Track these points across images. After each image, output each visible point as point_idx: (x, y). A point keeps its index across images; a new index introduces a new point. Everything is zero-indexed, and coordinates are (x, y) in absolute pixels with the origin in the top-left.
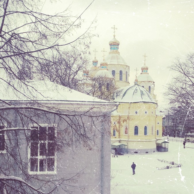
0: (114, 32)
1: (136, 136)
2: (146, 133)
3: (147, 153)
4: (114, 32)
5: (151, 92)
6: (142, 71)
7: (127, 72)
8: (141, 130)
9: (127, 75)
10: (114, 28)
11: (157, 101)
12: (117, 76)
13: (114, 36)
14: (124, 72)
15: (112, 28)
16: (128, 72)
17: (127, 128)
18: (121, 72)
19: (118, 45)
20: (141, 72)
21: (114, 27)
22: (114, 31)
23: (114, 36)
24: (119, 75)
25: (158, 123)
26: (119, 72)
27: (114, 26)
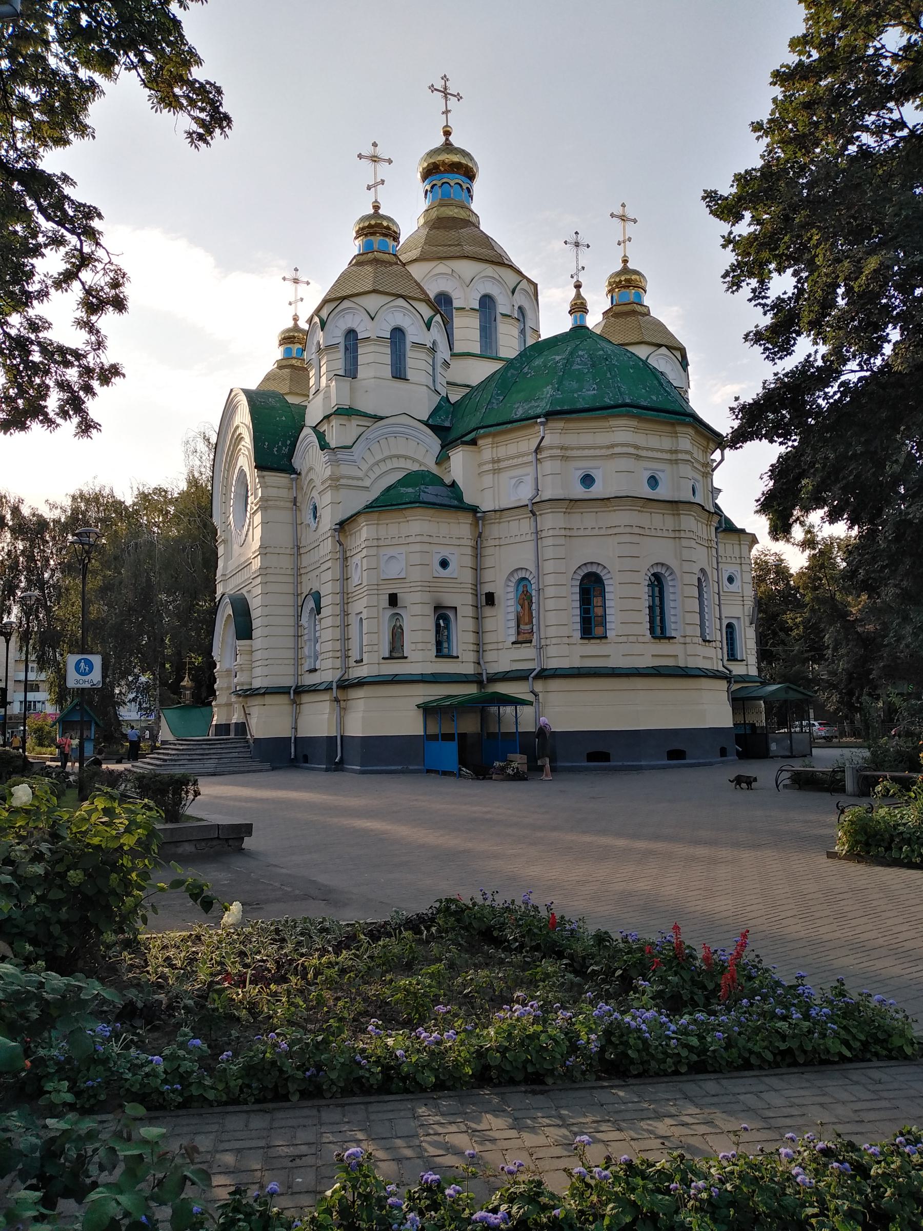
0: (447, 112)
1: (593, 647)
2: (659, 628)
3: (676, 755)
4: (447, 112)
8: (625, 606)
10: (445, 93)
13: (447, 133)
14: (503, 305)
15: (433, 88)
16: (529, 313)
18: (487, 302)
19: (470, 174)
21: (446, 88)
22: (444, 109)
23: (447, 133)
24: (474, 322)
25: (731, 580)
27: (444, 78)
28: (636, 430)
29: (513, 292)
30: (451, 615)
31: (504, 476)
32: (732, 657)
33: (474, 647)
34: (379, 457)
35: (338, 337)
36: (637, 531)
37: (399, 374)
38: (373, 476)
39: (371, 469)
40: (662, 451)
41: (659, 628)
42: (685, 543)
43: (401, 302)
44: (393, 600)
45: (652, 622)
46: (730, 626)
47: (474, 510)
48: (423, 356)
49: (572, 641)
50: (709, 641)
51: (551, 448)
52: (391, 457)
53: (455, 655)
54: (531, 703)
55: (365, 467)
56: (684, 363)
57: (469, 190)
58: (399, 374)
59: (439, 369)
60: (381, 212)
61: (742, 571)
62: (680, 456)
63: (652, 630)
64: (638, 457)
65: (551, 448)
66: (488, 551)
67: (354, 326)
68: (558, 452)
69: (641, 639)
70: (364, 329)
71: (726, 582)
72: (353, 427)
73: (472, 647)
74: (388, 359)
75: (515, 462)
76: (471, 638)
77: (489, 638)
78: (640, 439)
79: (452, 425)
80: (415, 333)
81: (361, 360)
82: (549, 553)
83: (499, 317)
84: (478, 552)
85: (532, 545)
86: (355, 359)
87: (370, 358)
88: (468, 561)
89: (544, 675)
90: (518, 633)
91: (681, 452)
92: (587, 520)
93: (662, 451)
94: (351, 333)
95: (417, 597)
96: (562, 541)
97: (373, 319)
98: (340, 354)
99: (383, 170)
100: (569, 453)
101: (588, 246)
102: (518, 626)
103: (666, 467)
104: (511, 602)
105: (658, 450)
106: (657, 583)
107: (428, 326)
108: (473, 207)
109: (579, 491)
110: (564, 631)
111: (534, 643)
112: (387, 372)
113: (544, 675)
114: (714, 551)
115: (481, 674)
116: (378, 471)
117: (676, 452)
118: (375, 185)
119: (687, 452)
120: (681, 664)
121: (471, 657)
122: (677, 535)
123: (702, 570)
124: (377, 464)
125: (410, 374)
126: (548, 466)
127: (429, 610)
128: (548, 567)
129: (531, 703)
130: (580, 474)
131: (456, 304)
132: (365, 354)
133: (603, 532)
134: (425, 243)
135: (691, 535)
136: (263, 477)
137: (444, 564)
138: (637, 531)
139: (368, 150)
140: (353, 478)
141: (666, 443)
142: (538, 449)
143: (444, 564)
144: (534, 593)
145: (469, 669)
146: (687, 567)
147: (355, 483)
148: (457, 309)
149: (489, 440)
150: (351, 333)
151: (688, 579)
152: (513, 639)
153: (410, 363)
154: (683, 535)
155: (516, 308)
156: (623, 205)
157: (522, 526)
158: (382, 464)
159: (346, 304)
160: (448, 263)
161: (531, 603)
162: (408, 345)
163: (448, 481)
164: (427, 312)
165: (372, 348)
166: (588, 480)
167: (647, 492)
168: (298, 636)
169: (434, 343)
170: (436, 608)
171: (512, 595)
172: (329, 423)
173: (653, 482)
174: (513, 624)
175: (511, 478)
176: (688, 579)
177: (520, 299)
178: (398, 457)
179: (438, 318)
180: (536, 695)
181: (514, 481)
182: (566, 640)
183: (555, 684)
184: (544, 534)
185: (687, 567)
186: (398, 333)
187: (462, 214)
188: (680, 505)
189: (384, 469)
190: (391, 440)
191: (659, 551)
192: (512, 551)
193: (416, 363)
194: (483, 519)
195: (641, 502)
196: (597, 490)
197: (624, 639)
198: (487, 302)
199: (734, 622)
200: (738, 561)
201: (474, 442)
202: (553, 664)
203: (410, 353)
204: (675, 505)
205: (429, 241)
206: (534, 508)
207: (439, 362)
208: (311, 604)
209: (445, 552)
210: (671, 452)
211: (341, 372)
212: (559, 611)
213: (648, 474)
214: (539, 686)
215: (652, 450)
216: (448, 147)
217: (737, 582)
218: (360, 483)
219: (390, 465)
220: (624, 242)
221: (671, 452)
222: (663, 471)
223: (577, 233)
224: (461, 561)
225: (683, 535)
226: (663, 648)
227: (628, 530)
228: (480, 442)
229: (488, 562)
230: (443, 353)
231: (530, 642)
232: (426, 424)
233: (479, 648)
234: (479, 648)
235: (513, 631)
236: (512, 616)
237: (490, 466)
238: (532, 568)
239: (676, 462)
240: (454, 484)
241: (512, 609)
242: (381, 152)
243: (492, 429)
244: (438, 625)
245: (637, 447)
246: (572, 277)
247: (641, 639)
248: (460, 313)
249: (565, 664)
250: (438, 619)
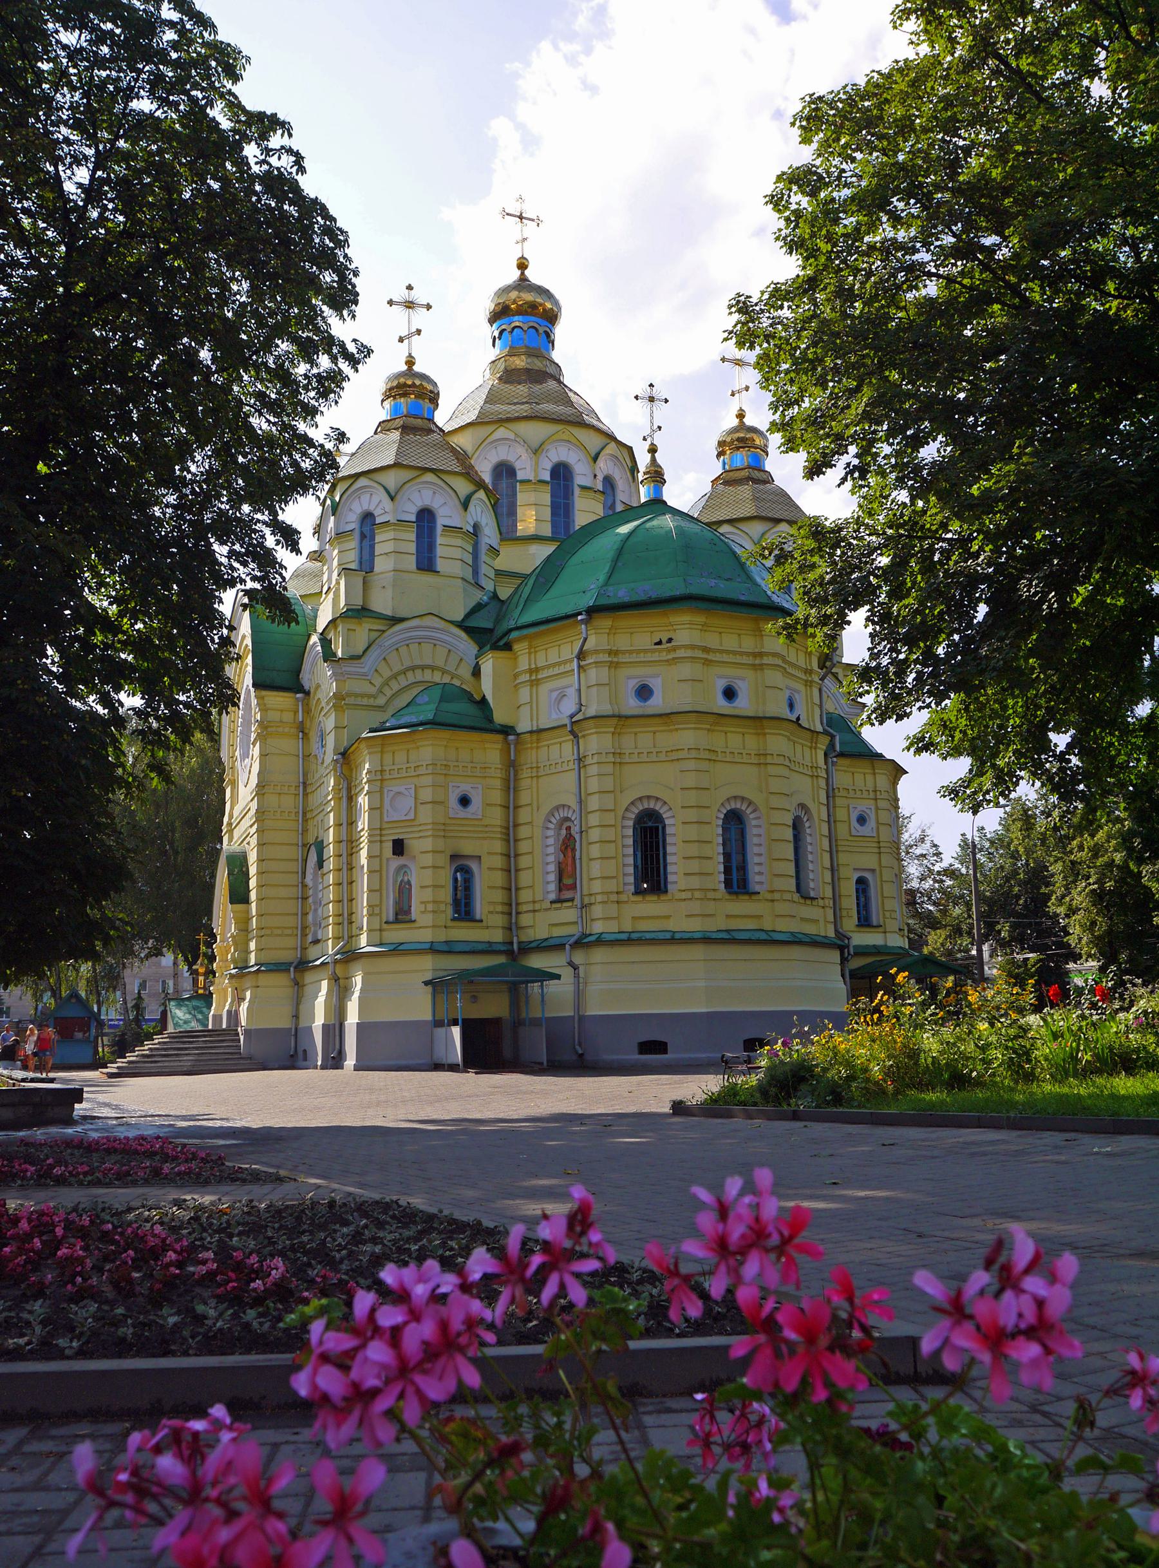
2: (737, 880)
8: (691, 853)
14: (582, 475)
17: (569, 837)
18: (561, 474)
25: (862, 820)
26: (547, 477)
28: (705, 628)
29: (595, 459)
30: (474, 866)
31: (544, 688)
32: (865, 922)
33: (506, 909)
34: (397, 668)
35: (352, 520)
36: (706, 755)
37: (426, 562)
38: (389, 693)
39: (386, 683)
40: (742, 654)
41: (737, 880)
42: (772, 770)
43: (430, 477)
44: (399, 847)
45: (727, 871)
46: (861, 881)
47: (506, 730)
48: (459, 542)
49: (623, 897)
50: (813, 899)
51: (596, 652)
52: (413, 668)
53: (478, 917)
54: (558, 977)
55: (378, 681)
57: (548, 335)
58: (426, 562)
59: (484, 557)
60: (416, 368)
61: (877, 808)
62: (766, 660)
63: (728, 883)
64: (707, 662)
65: (596, 652)
66: (524, 783)
67: (372, 508)
68: (606, 658)
69: (711, 895)
70: (383, 510)
71: (854, 823)
72: (363, 632)
73: (499, 908)
74: (412, 548)
75: (556, 671)
76: (499, 896)
77: (525, 896)
79: (489, 629)
80: (447, 514)
81: (378, 549)
82: (593, 785)
83: (577, 491)
84: (511, 785)
85: (573, 776)
86: (372, 547)
87: (389, 547)
88: (497, 797)
89: (582, 943)
90: (560, 890)
91: (767, 654)
92: (642, 740)
93: (742, 654)
94: (367, 517)
95: (428, 844)
96: (609, 769)
97: (392, 499)
98: (353, 543)
99: (420, 318)
100: (622, 658)
101: (666, 401)
102: (560, 880)
103: (749, 674)
104: (551, 850)
105: (734, 653)
106: (734, 821)
107: (465, 505)
108: (556, 355)
109: (632, 705)
110: (612, 886)
111: (577, 902)
112: (411, 562)
113: (582, 943)
114: (822, 783)
115: (511, 943)
116: (395, 686)
118: (409, 336)
119: (775, 655)
120: (767, 926)
121: (499, 920)
122: (762, 760)
123: (802, 806)
124: (395, 677)
125: (440, 565)
126: (593, 675)
127: (443, 860)
128: (594, 803)
129: (558, 977)
130: (633, 684)
131: (520, 475)
132: (384, 542)
133: (662, 757)
134: (486, 402)
135: (781, 760)
136: (263, 698)
137: (465, 801)
138: (706, 755)
139: (400, 294)
140: (363, 696)
142: (581, 655)
143: (465, 801)
144: (577, 837)
145: (497, 936)
146: (776, 802)
147: (365, 701)
148: (522, 482)
149: (525, 644)
150: (367, 517)
151: (778, 817)
152: (553, 896)
153: (440, 551)
154: (769, 759)
155: (600, 477)
157: (562, 750)
158: (401, 678)
159: (363, 481)
160: (511, 426)
161: (574, 850)
162: (439, 529)
163: (478, 698)
164: (463, 487)
165: (390, 535)
166: (644, 692)
167: (721, 704)
168: (305, 899)
169: (476, 526)
170: (454, 857)
171: (551, 841)
172: (336, 628)
173: (730, 694)
174: (552, 877)
175: (552, 691)
176: (778, 817)
177: (604, 466)
178: (423, 668)
179: (481, 494)
180: (575, 968)
181: (555, 694)
182: (614, 897)
183: (599, 955)
184: (589, 760)
185: (776, 802)
186: (426, 517)
187: (538, 364)
188: (765, 722)
189: (404, 683)
190: (414, 647)
191: (737, 781)
192: (553, 782)
193: (450, 552)
194: (517, 743)
195: (711, 719)
196: (657, 703)
197: (688, 895)
198: (561, 474)
199: (867, 875)
200: (872, 795)
201: (508, 647)
202: (598, 928)
203: (440, 540)
204: (758, 722)
205: (491, 398)
206: (575, 728)
207: (483, 549)
208: (313, 858)
209: (465, 787)
210: (755, 655)
211: (353, 566)
212: (608, 860)
213: (721, 684)
214: (579, 957)
215: (728, 652)
216: (523, 283)
217: (871, 823)
218: (371, 701)
219: (411, 677)
222: (743, 679)
223: (651, 385)
224: (488, 798)
225: (769, 759)
226: (741, 905)
227: (694, 754)
228: (516, 647)
229: (524, 798)
230: (490, 534)
231: (572, 900)
232: (460, 625)
233: (511, 908)
234: (511, 908)
235: (552, 887)
236: (552, 868)
237: (526, 677)
238: (574, 805)
239: (760, 667)
240: (483, 701)
241: (551, 858)
242: (419, 296)
243: (525, 632)
244: (456, 880)
245: (706, 650)
246: (645, 439)
247: (711, 895)
248: (525, 487)
249: (612, 927)
250: (456, 871)
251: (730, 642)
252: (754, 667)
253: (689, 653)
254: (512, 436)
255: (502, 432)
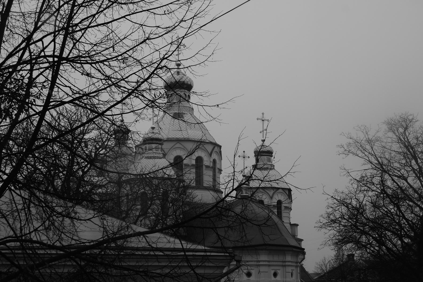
5: (285, 220)
6: (257, 161)
7: (214, 161)
9: (217, 171)
11: (302, 240)
12: (190, 176)
14: (207, 161)
16: (218, 161)
18: (199, 160)
20: (253, 161)
26: (194, 162)
29: (211, 155)
40: (279, 261)
56: (290, 196)
62: (287, 264)
64: (269, 266)
78: (270, 258)
83: (204, 167)
101: (249, 157)
117: (285, 262)
141: (281, 258)
156: (263, 114)
198: (199, 160)
210: (283, 262)
213: (273, 272)
220: (263, 131)
221: (283, 262)
222: (279, 270)
239: (285, 266)
245: (269, 261)
251: (276, 258)
252: (283, 266)
253: (264, 263)
254: (181, 146)
255: (178, 145)
